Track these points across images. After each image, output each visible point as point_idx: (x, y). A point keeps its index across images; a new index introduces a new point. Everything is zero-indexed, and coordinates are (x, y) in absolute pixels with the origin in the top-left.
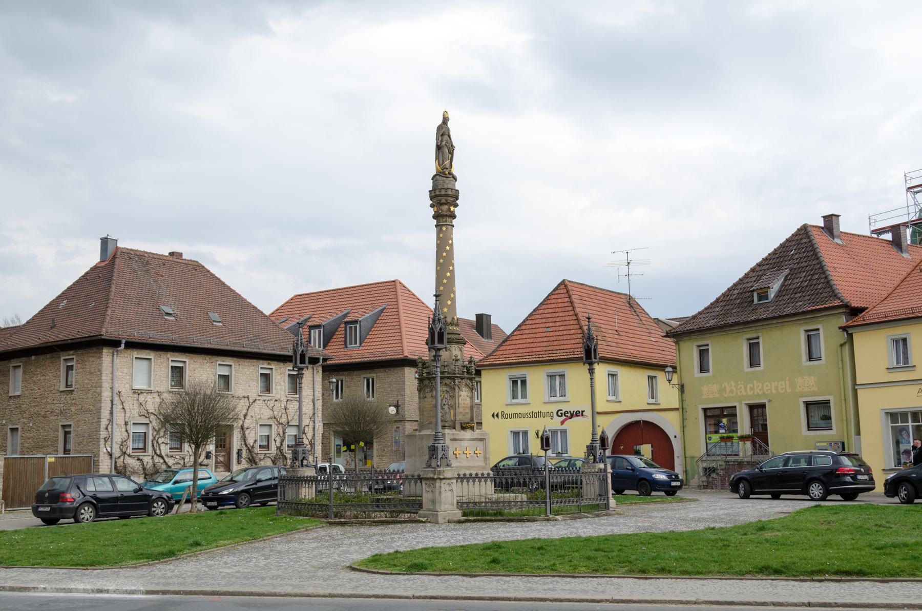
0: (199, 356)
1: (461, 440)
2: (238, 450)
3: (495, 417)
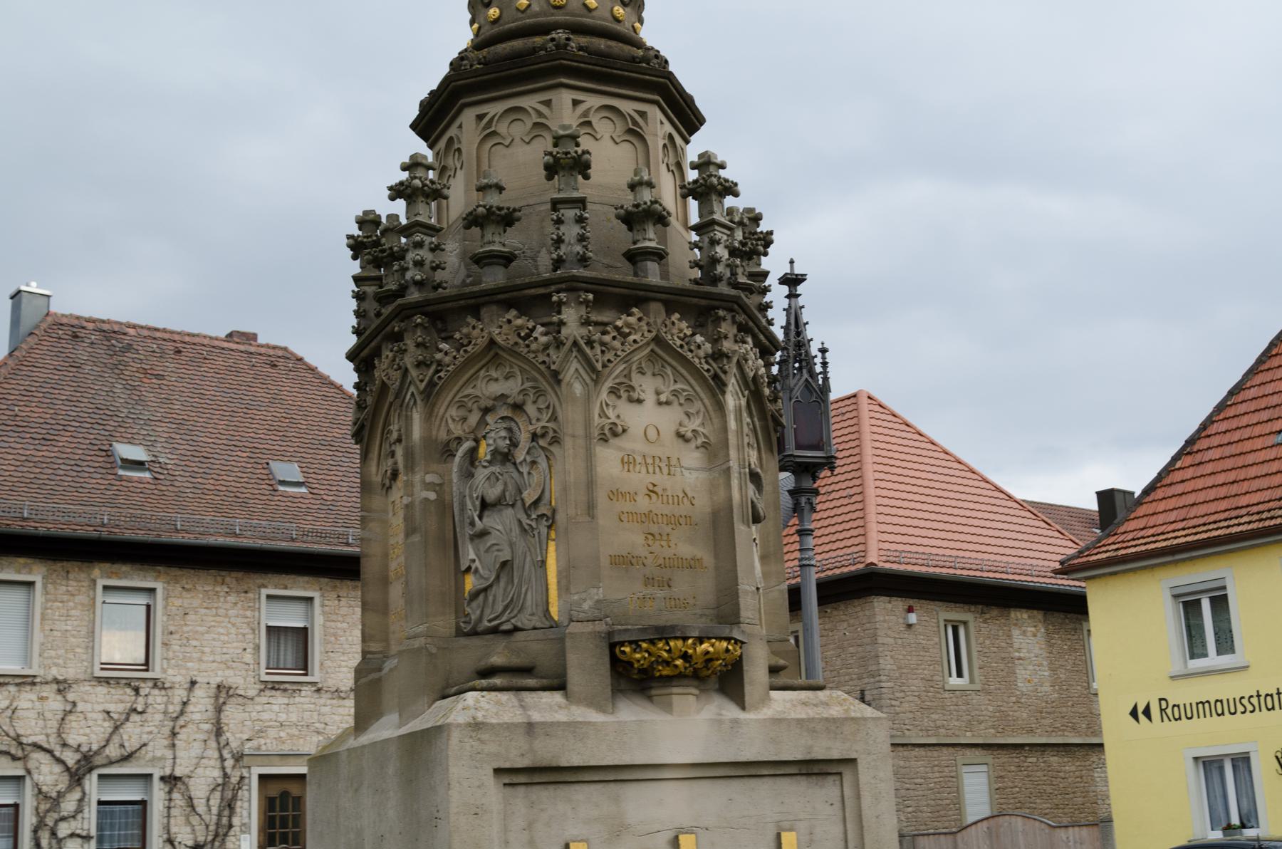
0: (202, 573)
3: (1141, 717)
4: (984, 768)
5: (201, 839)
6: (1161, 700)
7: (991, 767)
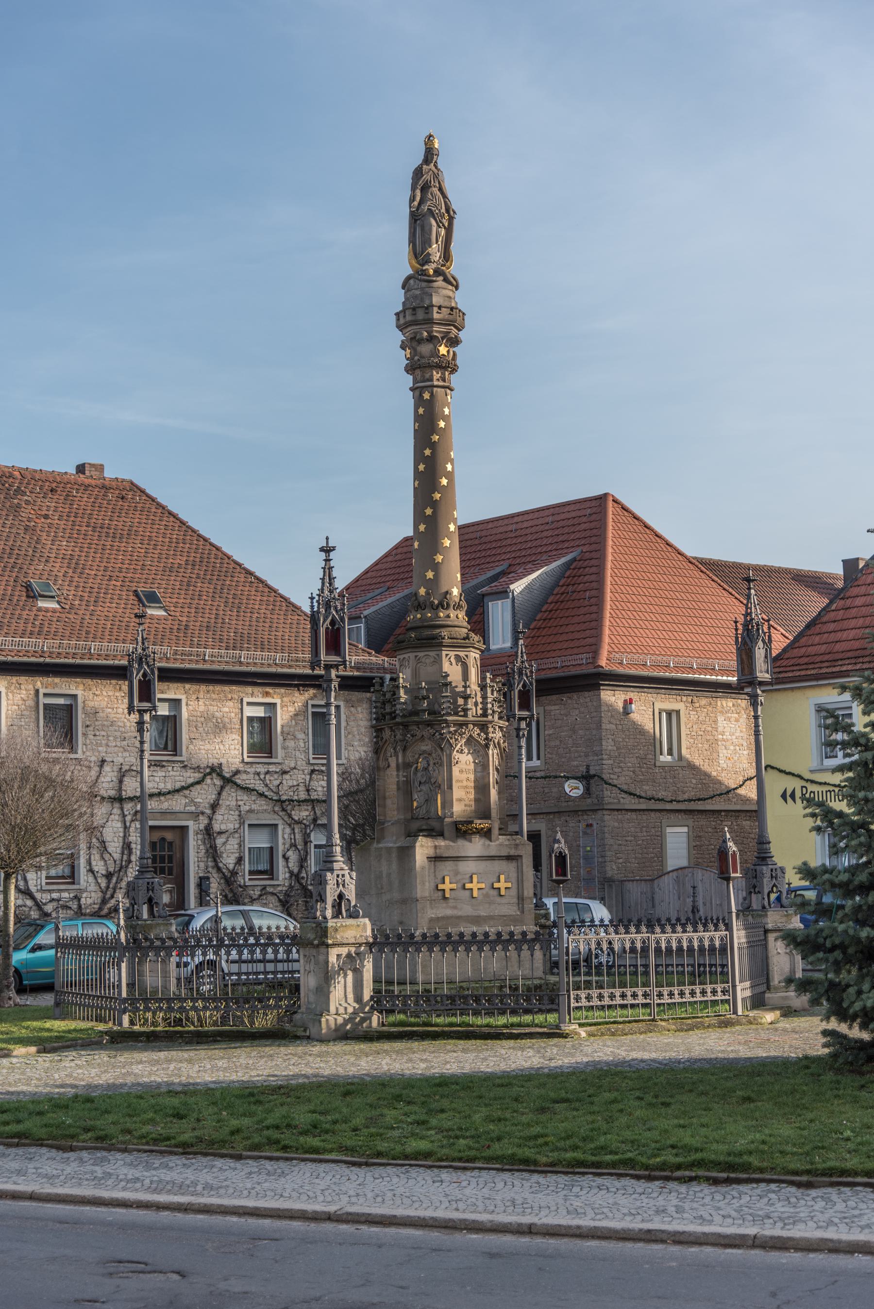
1: (457, 859)
2: (201, 878)
3: (789, 798)
4: (685, 829)
5: (111, 870)
6: (802, 787)
7: (691, 828)
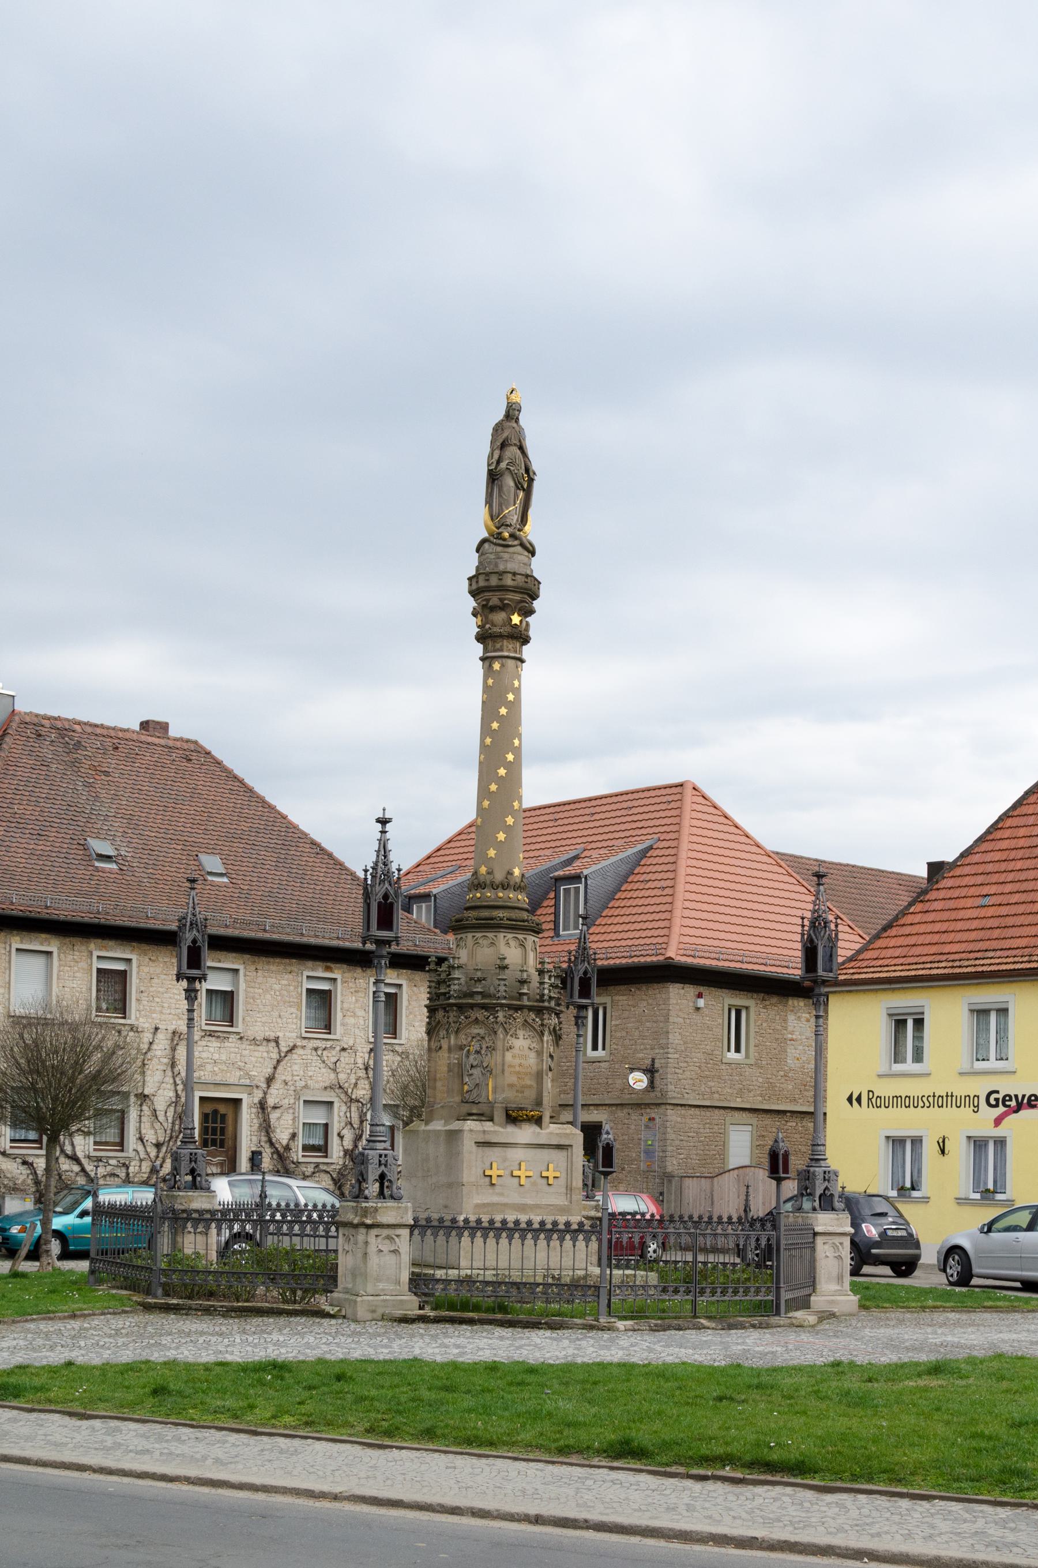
0: (161, 948)
2: (253, 1153)
3: (855, 1102)
4: (749, 1128)
5: (161, 1139)
6: (869, 1091)
7: (755, 1128)
